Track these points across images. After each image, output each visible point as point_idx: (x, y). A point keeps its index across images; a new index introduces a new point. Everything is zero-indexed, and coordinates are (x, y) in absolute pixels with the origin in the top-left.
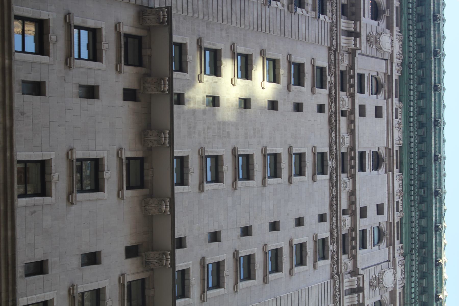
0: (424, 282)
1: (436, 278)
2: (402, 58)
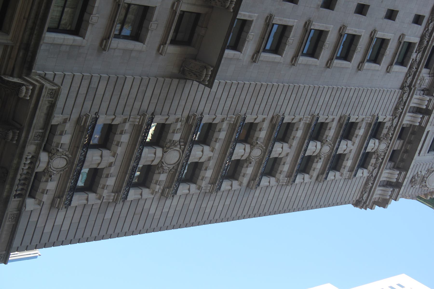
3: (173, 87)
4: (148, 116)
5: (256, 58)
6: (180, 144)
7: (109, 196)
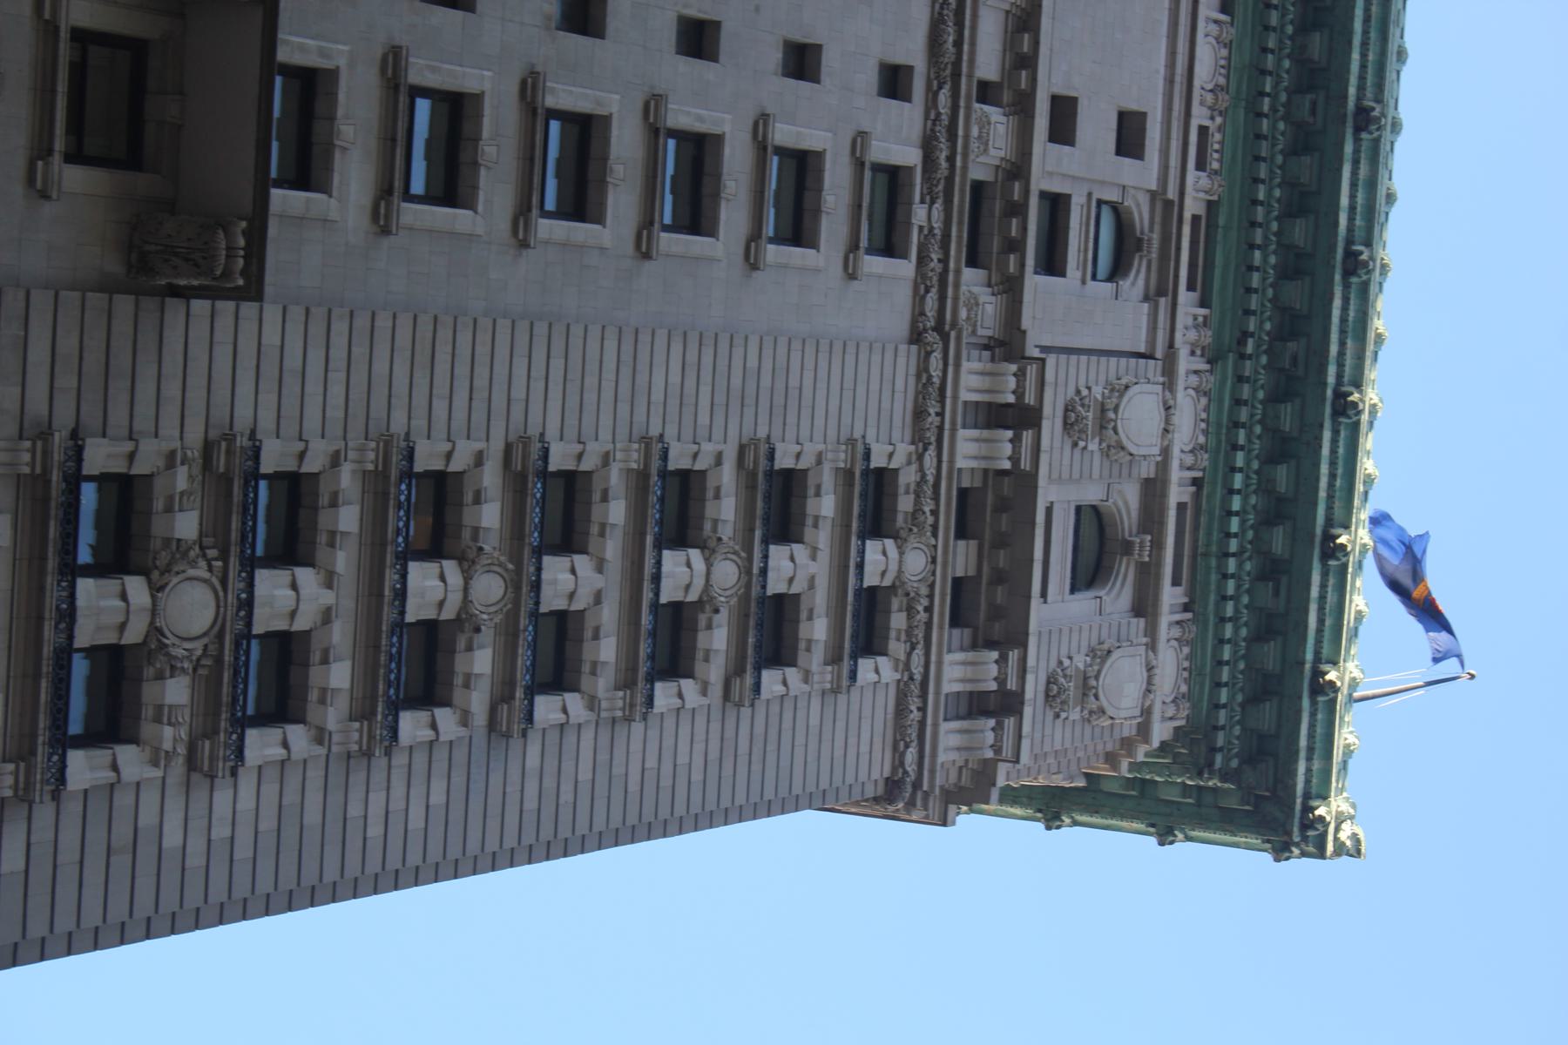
0: (1282, 475)
1: (1333, 463)
3: (122, 325)
4: (59, 438)
5: (387, 217)
6: (204, 556)
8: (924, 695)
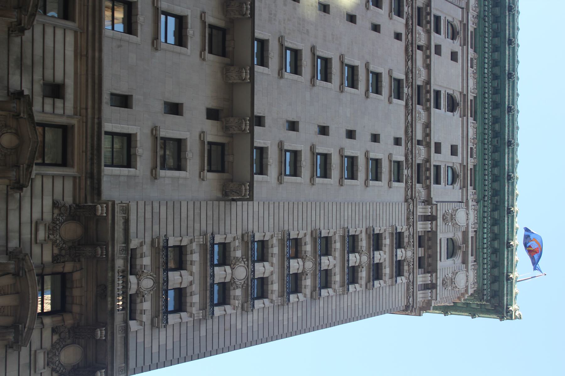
0: (496, 228)
1: (508, 225)
2: (478, 11)
3: (222, 208)
4: (209, 235)
6: (243, 260)
7: (198, 313)
8: (413, 285)
